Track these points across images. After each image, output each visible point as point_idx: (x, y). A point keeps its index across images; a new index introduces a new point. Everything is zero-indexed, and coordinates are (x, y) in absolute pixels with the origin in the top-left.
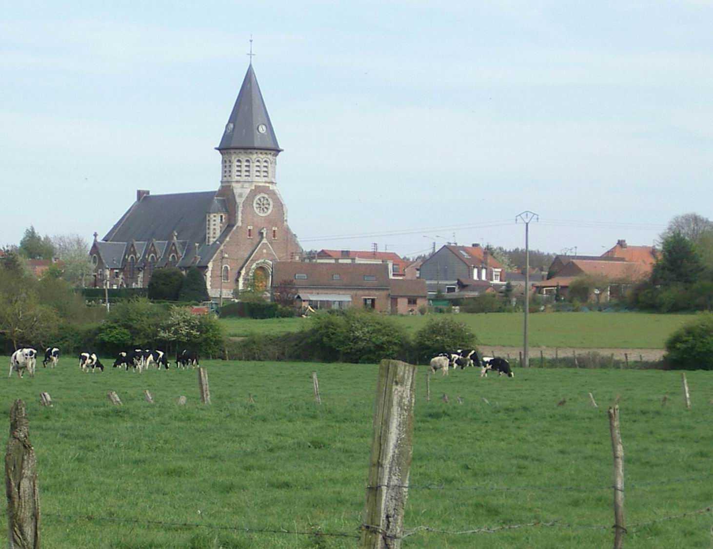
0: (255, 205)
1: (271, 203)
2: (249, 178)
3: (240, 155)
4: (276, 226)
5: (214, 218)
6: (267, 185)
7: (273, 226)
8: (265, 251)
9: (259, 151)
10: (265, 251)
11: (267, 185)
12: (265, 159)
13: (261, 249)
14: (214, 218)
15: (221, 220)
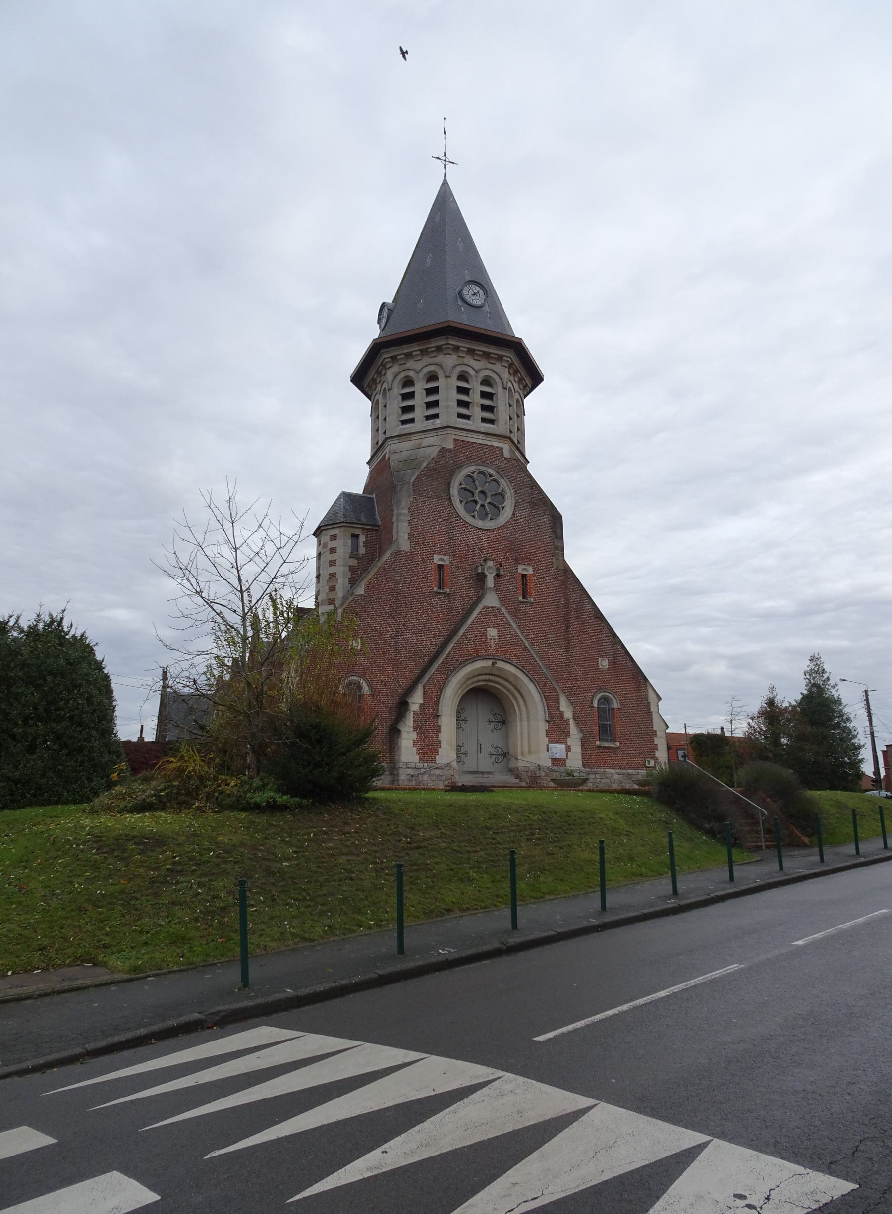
0: (454, 491)
1: (509, 493)
2: (438, 421)
3: (411, 364)
4: (529, 560)
6: (496, 443)
7: (518, 561)
8: (492, 632)
9: (464, 344)
10: (492, 632)
11: (496, 443)
12: (488, 373)
13: (483, 624)
15: (355, 547)
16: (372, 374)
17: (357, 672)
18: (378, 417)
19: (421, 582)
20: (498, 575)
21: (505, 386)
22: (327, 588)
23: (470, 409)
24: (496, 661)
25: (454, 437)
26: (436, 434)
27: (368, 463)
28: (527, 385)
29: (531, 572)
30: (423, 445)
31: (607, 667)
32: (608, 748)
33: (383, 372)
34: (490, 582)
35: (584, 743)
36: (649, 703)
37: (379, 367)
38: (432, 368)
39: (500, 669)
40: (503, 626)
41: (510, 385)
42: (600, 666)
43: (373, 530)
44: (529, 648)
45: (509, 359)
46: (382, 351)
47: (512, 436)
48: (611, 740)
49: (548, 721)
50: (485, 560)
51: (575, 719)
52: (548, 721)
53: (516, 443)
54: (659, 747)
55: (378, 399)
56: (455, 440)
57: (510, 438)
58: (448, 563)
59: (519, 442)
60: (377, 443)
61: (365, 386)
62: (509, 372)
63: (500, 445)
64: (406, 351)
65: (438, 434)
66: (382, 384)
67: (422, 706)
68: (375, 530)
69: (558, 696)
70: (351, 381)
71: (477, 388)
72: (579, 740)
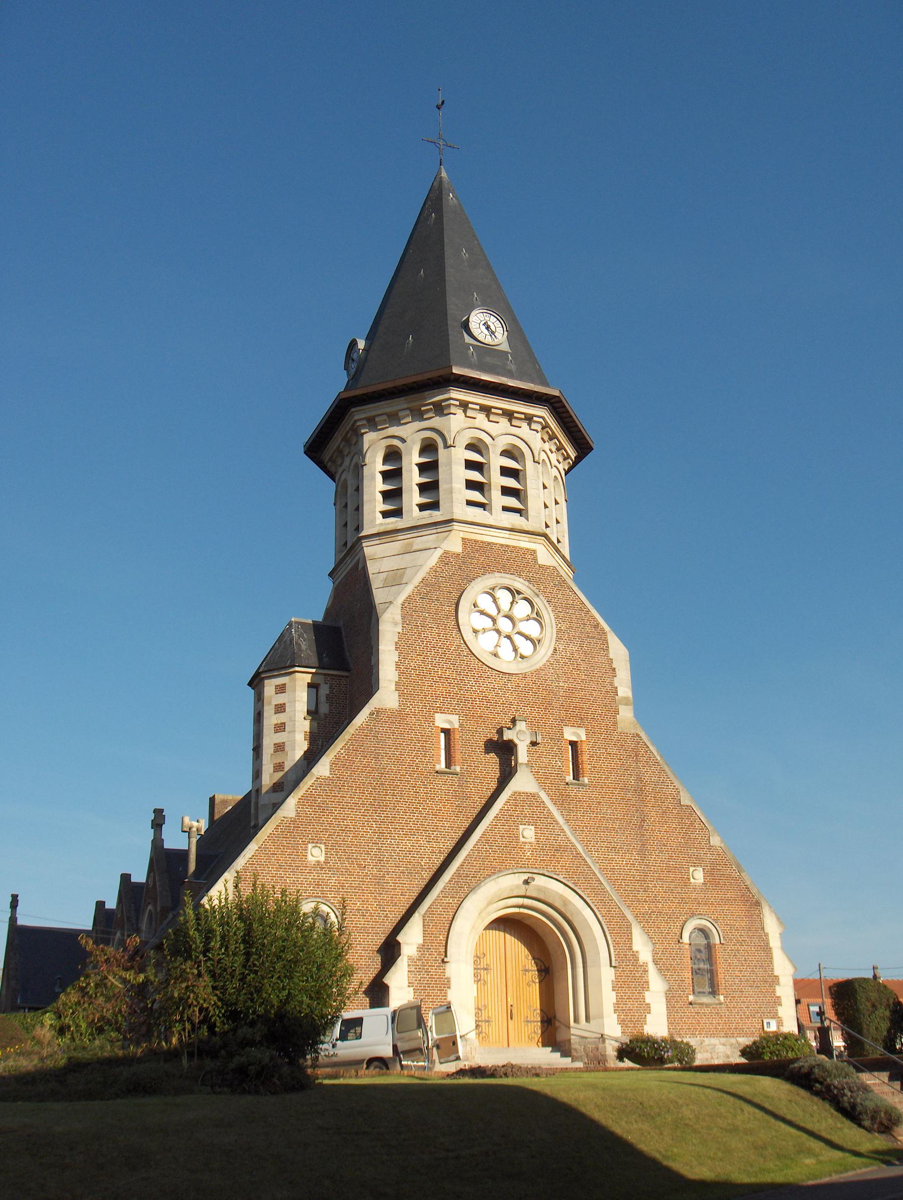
2: (435, 513)
4: (579, 721)
5: (280, 699)
6: (524, 542)
7: (563, 722)
8: (528, 833)
11: (524, 542)
13: (510, 819)
14: (280, 699)
16: (337, 441)
17: (320, 897)
18: (346, 506)
19: (417, 756)
20: (534, 744)
21: (536, 459)
22: (272, 766)
23: (486, 493)
24: (534, 876)
25: (462, 535)
26: (435, 531)
27: (330, 575)
28: (568, 457)
29: (584, 738)
30: (415, 548)
31: (702, 881)
32: (708, 1005)
33: (354, 441)
34: (522, 754)
35: (671, 998)
36: (767, 935)
37: (348, 432)
38: (428, 434)
39: (540, 889)
40: (542, 820)
41: (543, 456)
42: (692, 880)
43: (340, 676)
44: (583, 854)
45: (541, 420)
46: (353, 410)
47: (548, 531)
48: (710, 993)
49: (615, 967)
50: (514, 721)
51: (655, 962)
52: (615, 967)
53: (556, 542)
54: (784, 1001)
55: (345, 480)
56: (463, 538)
57: (545, 536)
58: (457, 726)
59: (559, 541)
60: (346, 544)
61: (327, 460)
62: (542, 439)
63: (532, 546)
64: (388, 410)
65: (439, 530)
66: (352, 459)
67: (422, 948)
68: (343, 676)
69: (629, 927)
70: (305, 453)
71: (497, 461)
72: (663, 995)
